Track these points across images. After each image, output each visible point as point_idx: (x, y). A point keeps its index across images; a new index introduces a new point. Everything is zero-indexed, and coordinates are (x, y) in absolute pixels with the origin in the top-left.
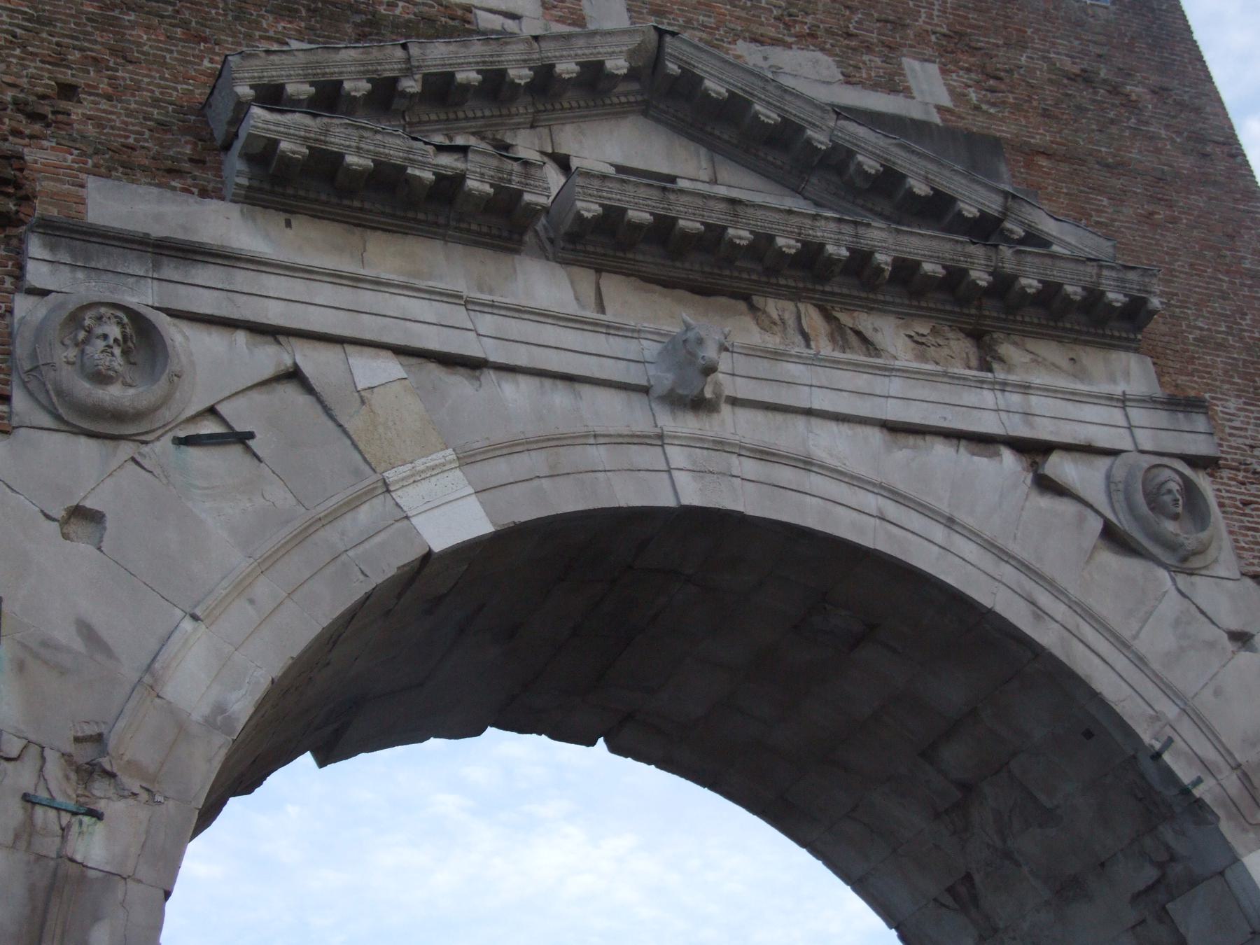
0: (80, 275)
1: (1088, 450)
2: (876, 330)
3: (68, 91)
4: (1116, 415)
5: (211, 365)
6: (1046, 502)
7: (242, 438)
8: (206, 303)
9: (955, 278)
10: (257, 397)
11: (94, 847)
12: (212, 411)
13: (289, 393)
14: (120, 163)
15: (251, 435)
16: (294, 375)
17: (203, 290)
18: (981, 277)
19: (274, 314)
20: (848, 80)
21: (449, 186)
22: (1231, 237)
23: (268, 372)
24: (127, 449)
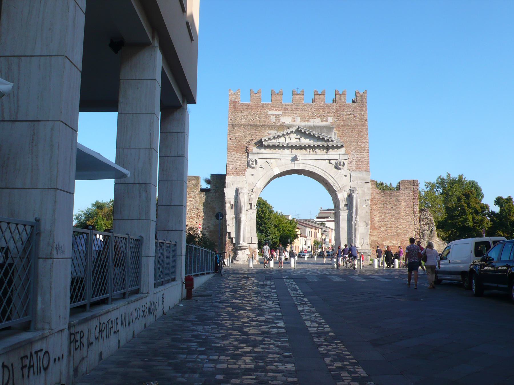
6: (330, 164)
9: (323, 146)
11: (252, 196)
17: (260, 156)
18: (326, 146)
21: (278, 146)
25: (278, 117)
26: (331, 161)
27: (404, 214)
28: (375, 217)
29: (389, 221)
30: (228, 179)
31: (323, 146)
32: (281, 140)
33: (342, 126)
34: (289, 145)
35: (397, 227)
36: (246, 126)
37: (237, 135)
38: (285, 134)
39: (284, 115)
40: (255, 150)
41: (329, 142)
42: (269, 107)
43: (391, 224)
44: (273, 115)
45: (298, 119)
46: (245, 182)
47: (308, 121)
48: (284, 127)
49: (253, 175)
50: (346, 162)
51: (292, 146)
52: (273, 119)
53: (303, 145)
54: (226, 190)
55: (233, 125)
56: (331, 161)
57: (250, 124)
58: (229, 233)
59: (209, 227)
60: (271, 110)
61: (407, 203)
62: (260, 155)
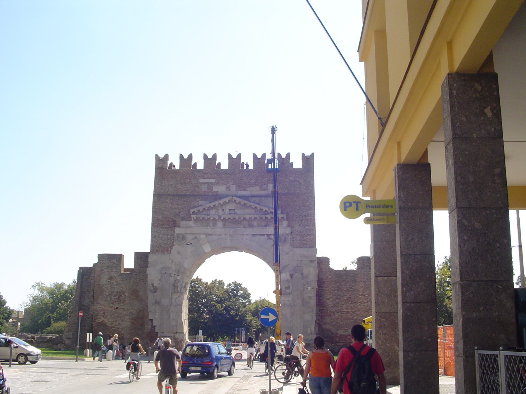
3: (180, 212)
5: (189, 238)
11: (178, 278)
14: (183, 219)
16: (196, 237)
18: (264, 218)
19: (194, 233)
20: (261, 190)
25: (210, 186)
27: (363, 297)
28: (328, 301)
29: (345, 306)
30: (151, 258)
31: (261, 218)
32: (213, 212)
33: (284, 195)
34: (222, 218)
35: (354, 312)
36: (173, 195)
38: (217, 205)
39: (218, 184)
40: (183, 223)
41: (268, 214)
43: (346, 309)
45: (233, 187)
46: (171, 261)
47: (245, 190)
48: (217, 197)
49: (178, 253)
50: (289, 237)
51: (224, 218)
52: (204, 188)
53: (237, 218)
54: (149, 271)
55: (159, 195)
58: (152, 320)
59: (131, 313)
60: (202, 177)
61: (365, 284)
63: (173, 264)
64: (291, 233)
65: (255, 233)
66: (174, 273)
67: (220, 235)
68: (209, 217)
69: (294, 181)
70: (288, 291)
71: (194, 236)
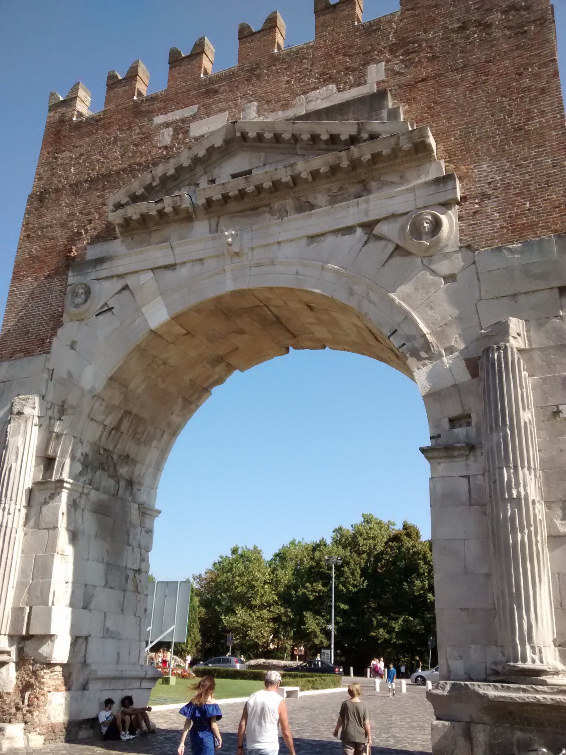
0: (79, 277)
1: (393, 216)
2: (315, 199)
3: (90, 222)
4: (411, 196)
7: (110, 309)
8: (104, 273)
10: (117, 296)
12: (106, 304)
13: (126, 292)
14: (97, 239)
15: (113, 308)
16: (126, 287)
17: (105, 270)
18: (345, 164)
20: (339, 90)
22: (520, 74)
23: (119, 289)
24: (85, 322)
26: (382, 229)
31: (334, 169)
33: (424, 80)
37: (47, 219)
42: (157, 105)
44: (167, 125)
46: (46, 376)
47: (285, 106)
49: (73, 345)
56: (382, 229)
57: (94, 174)
60: (164, 111)
62: (106, 265)
63: (51, 384)
64: (464, 198)
65: (318, 231)
66: (50, 413)
67: (201, 260)
68: (159, 206)
69: (464, 28)
70: (460, 432)
71: (119, 284)
